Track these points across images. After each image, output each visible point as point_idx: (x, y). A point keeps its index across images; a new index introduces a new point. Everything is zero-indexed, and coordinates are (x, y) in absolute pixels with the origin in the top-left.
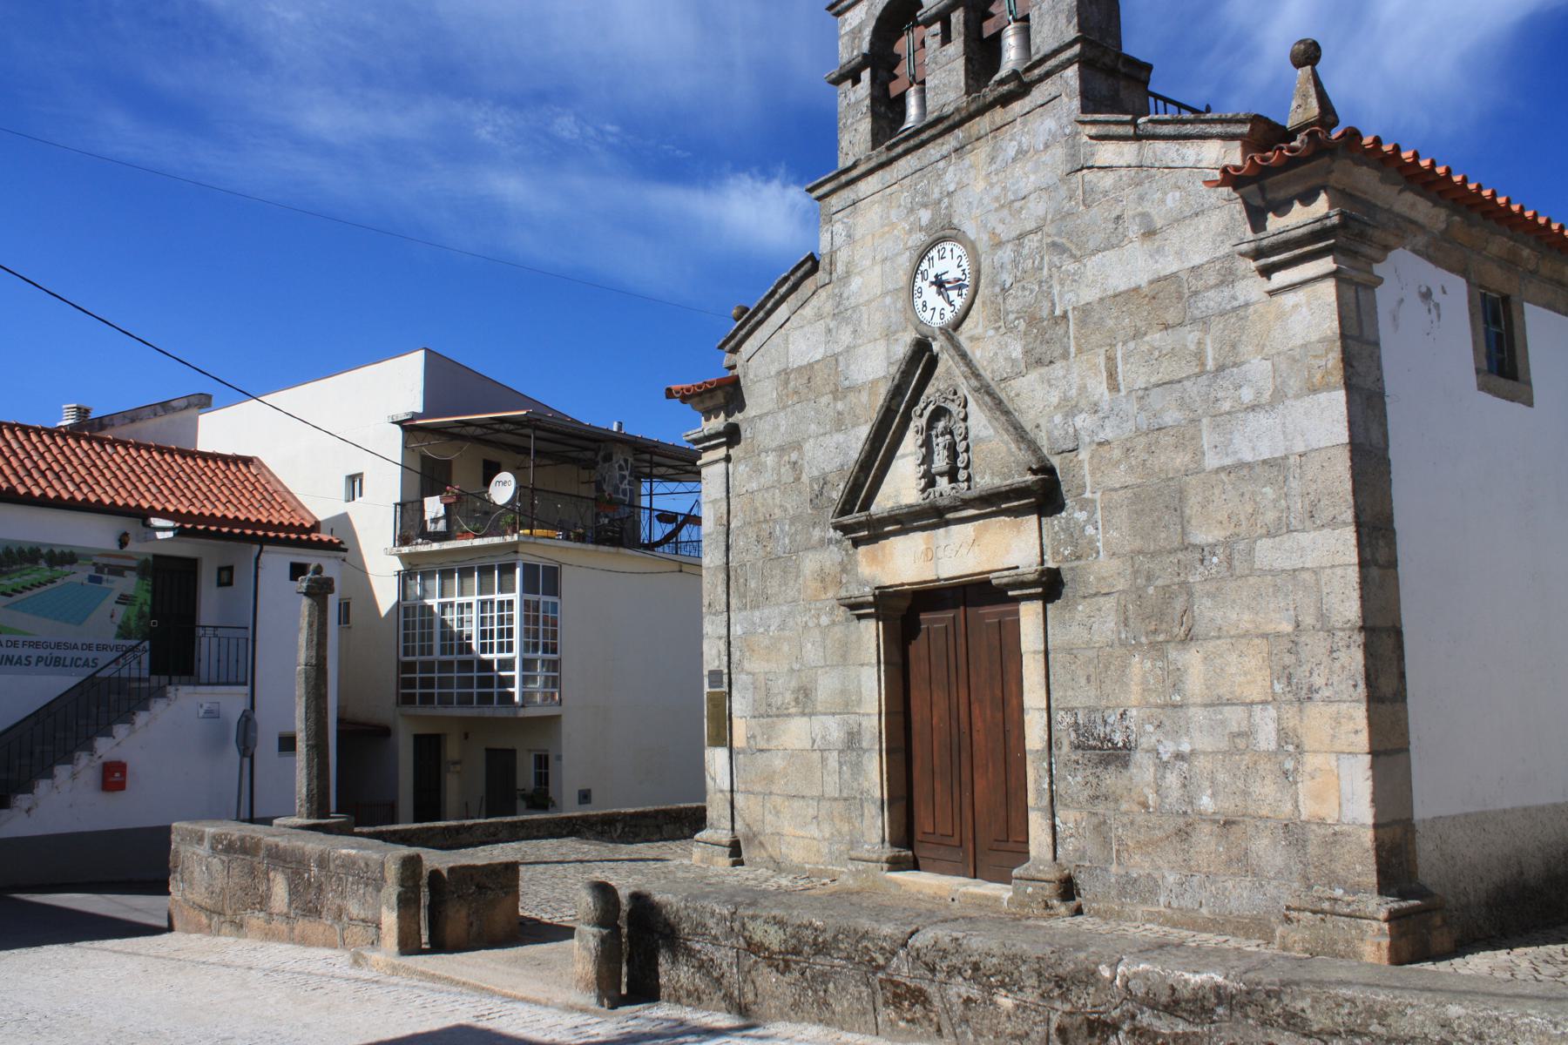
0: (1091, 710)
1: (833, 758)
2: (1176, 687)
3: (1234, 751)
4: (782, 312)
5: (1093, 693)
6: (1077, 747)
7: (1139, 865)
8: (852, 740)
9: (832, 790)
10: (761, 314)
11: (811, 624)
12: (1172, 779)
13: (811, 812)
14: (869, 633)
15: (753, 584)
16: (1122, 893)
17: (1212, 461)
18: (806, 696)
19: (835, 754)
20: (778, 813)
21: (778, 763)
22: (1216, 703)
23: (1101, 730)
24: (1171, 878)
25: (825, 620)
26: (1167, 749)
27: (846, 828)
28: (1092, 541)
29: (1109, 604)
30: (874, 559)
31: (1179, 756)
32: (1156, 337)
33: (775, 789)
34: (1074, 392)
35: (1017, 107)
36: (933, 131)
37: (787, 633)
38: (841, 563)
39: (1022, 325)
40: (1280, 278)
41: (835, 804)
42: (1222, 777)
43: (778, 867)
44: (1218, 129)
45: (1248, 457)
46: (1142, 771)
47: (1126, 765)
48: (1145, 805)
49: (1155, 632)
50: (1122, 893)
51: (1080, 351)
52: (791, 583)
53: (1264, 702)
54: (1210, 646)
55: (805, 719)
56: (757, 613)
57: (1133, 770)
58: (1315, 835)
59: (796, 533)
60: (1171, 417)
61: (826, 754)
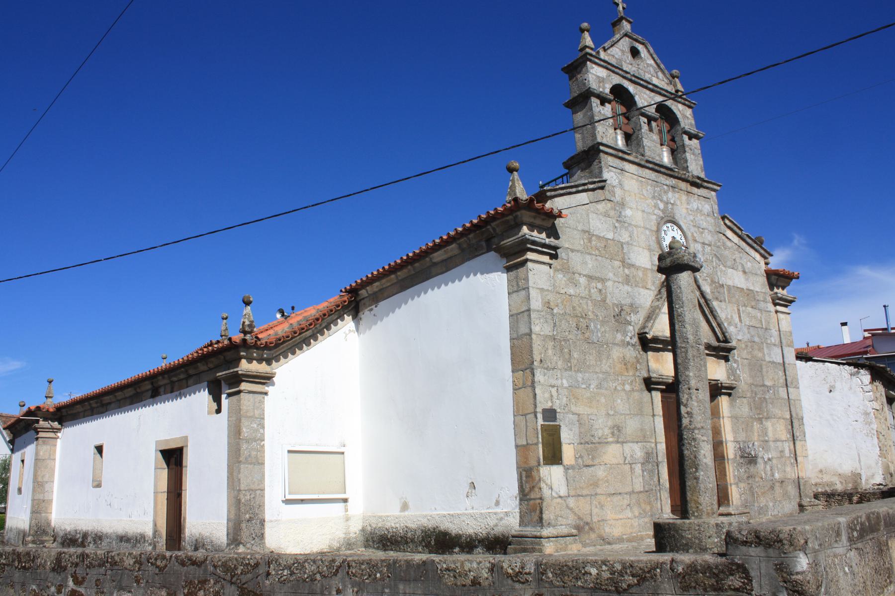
0: (744, 442)
1: (638, 468)
2: (766, 434)
3: (782, 457)
4: (583, 197)
7: (763, 501)
8: (649, 458)
9: (639, 487)
10: (574, 190)
11: (619, 388)
12: (768, 468)
13: (626, 502)
14: (657, 396)
15: (575, 355)
16: (760, 514)
17: (767, 359)
18: (619, 431)
19: (639, 465)
20: (602, 507)
21: (601, 472)
22: (776, 441)
23: (748, 450)
24: (771, 504)
25: (628, 388)
27: (648, 508)
28: (739, 376)
29: (745, 401)
30: (657, 360)
31: (769, 459)
32: (749, 309)
33: (599, 491)
35: (695, 190)
36: (666, 171)
37: (603, 391)
38: (636, 357)
39: (709, 280)
40: (779, 308)
41: (641, 495)
43: (605, 541)
44: (762, 252)
46: (760, 465)
50: (760, 514)
52: (604, 361)
54: (773, 420)
55: (618, 445)
56: (580, 376)
58: (802, 482)
59: (605, 331)
60: (756, 339)
61: (633, 466)
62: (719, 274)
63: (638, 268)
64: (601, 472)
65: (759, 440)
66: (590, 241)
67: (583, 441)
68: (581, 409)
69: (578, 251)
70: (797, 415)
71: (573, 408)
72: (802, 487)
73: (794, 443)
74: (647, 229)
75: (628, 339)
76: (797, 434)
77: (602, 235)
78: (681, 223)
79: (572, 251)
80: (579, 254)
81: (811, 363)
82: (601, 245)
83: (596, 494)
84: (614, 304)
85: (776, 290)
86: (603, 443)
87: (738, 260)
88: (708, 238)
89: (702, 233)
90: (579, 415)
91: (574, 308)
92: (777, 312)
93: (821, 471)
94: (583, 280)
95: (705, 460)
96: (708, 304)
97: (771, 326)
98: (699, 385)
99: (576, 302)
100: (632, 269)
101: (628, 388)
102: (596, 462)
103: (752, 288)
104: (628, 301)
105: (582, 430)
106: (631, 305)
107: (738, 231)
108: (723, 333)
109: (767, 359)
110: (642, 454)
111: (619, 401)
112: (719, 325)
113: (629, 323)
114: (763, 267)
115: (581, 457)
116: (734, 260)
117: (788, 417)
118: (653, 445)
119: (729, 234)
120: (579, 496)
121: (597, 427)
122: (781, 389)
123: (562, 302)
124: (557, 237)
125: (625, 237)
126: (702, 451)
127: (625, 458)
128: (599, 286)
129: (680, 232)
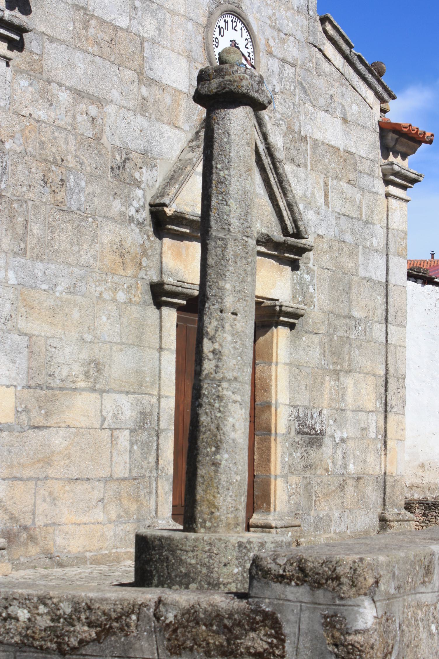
0: (306, 408)
1: (124, 438)
3: (363, 438)
5: (308, 397)
6: (299, 433)
7: (324, 508)
8: (145, 420)
9: (121, 469)
11: (105, 296)
12: (339, 454)
13: (97, 494)
15: (36, 229)
16: (316, 528)
17: (362, 273)
18: (98, 371)
19: (127, 433)
20: (54, 500)
21: (58, 440)
22: (357, 410)
23: (310, 422)
24: (337, 514)
25: (121, 296)
26: (338, 436)
27: (134, 507)
28: (312, 297)
29: (316, 339)
30: (178, 255)
31: (343, 440)
32: (344, 185)
33: (51, 472)
34: (309, 193)
37: (78, 298)
38: (142, 246)
39: (284, 127)
40: (392, 189)
41: (123, 485)
42: (357, 452)
43: (53, 559)
44: (380, 89)
45: (374, 277)
46: (327, 448)
47: (320, 445)
48: (327, 470)
49: (336, 363)
50: (316, 528)
51: (312, 169)
52: (85, 246)
53: (373, 412)
54: (357, 376)
55: (95, 395)
56: (40, 267)
57: (324, 448)
59: (94, 194)
60: (348, 238)
61: (116, 433)
62: (302, 117)
63: (165, 88)
64: (58, 440)
65: (330, 407)
66: (86, 26)
67: (32, 383)
68: (36, 327)
69: (61, 42)
70: (396, 370)
71: (22, 324)
72: (388, 490)
73: (386, 417)
74: (190, 19)
75: (132, 212)
76: (392, 402)
77: (108, 18)
78: (251, 19)
79: (52, 39)
80: (63, 47)
81: (430, 287)
82: (104, 36)
83: (46, 478)
84: (115, 147)
85: (391, 158)
86: (68, 389)
87: (337, 99)
88: (293, 51)
89: (284, 41)
90: (30, 337)
91: (42, 144)
92: (387, 195)
93: (422, 466)
94: (64, 96)
95: (233, 435)
96: (276, 168)
97: (376, 219)
98: (239, 307)
99: (47, 134)
100: (155, 89)
101: (121, 296)
102: (52, 422)
103: (353, 150)
104: (140, 145)
105: (34, 364)
106: (145, 153)
107: (344, 46)
108: (295, 221)
109: (362, 273)
110: (134, 414)
111: (104, 318)
112: (290, 206)
113: (138, 184)
114: (377, 115)
115: (27, 410)
116: (331, 96)
117: (382, 372)
118: (154, 400)
119: (329, 49)
120: (16, 478)
121: (61, 360)
122: (376, 326)
123: (22, 131)
124: (26, 10)
125: (149, 29)
126: (230, 419)
127: (104, 419)
128: (93, 110)
129: (246, 35)
